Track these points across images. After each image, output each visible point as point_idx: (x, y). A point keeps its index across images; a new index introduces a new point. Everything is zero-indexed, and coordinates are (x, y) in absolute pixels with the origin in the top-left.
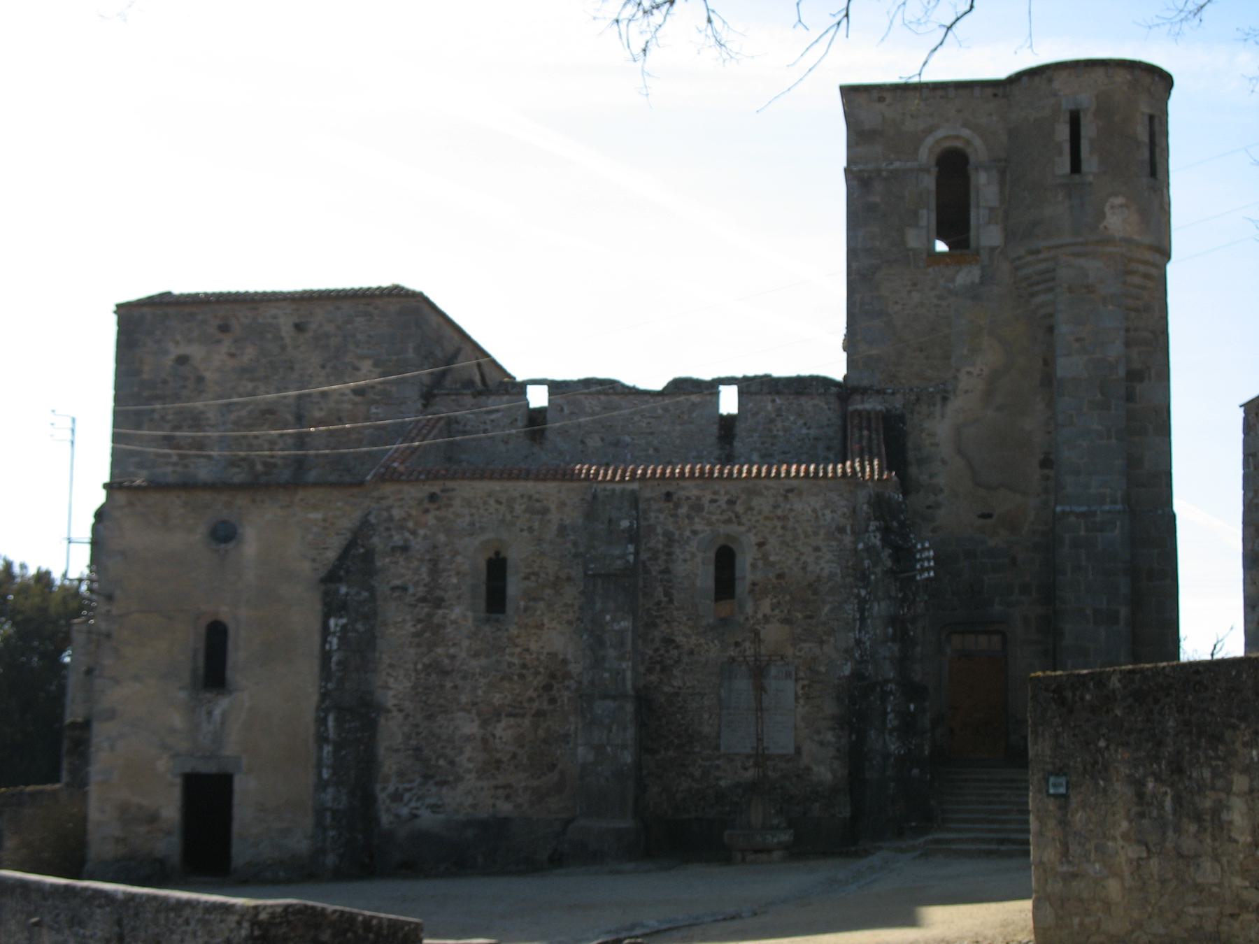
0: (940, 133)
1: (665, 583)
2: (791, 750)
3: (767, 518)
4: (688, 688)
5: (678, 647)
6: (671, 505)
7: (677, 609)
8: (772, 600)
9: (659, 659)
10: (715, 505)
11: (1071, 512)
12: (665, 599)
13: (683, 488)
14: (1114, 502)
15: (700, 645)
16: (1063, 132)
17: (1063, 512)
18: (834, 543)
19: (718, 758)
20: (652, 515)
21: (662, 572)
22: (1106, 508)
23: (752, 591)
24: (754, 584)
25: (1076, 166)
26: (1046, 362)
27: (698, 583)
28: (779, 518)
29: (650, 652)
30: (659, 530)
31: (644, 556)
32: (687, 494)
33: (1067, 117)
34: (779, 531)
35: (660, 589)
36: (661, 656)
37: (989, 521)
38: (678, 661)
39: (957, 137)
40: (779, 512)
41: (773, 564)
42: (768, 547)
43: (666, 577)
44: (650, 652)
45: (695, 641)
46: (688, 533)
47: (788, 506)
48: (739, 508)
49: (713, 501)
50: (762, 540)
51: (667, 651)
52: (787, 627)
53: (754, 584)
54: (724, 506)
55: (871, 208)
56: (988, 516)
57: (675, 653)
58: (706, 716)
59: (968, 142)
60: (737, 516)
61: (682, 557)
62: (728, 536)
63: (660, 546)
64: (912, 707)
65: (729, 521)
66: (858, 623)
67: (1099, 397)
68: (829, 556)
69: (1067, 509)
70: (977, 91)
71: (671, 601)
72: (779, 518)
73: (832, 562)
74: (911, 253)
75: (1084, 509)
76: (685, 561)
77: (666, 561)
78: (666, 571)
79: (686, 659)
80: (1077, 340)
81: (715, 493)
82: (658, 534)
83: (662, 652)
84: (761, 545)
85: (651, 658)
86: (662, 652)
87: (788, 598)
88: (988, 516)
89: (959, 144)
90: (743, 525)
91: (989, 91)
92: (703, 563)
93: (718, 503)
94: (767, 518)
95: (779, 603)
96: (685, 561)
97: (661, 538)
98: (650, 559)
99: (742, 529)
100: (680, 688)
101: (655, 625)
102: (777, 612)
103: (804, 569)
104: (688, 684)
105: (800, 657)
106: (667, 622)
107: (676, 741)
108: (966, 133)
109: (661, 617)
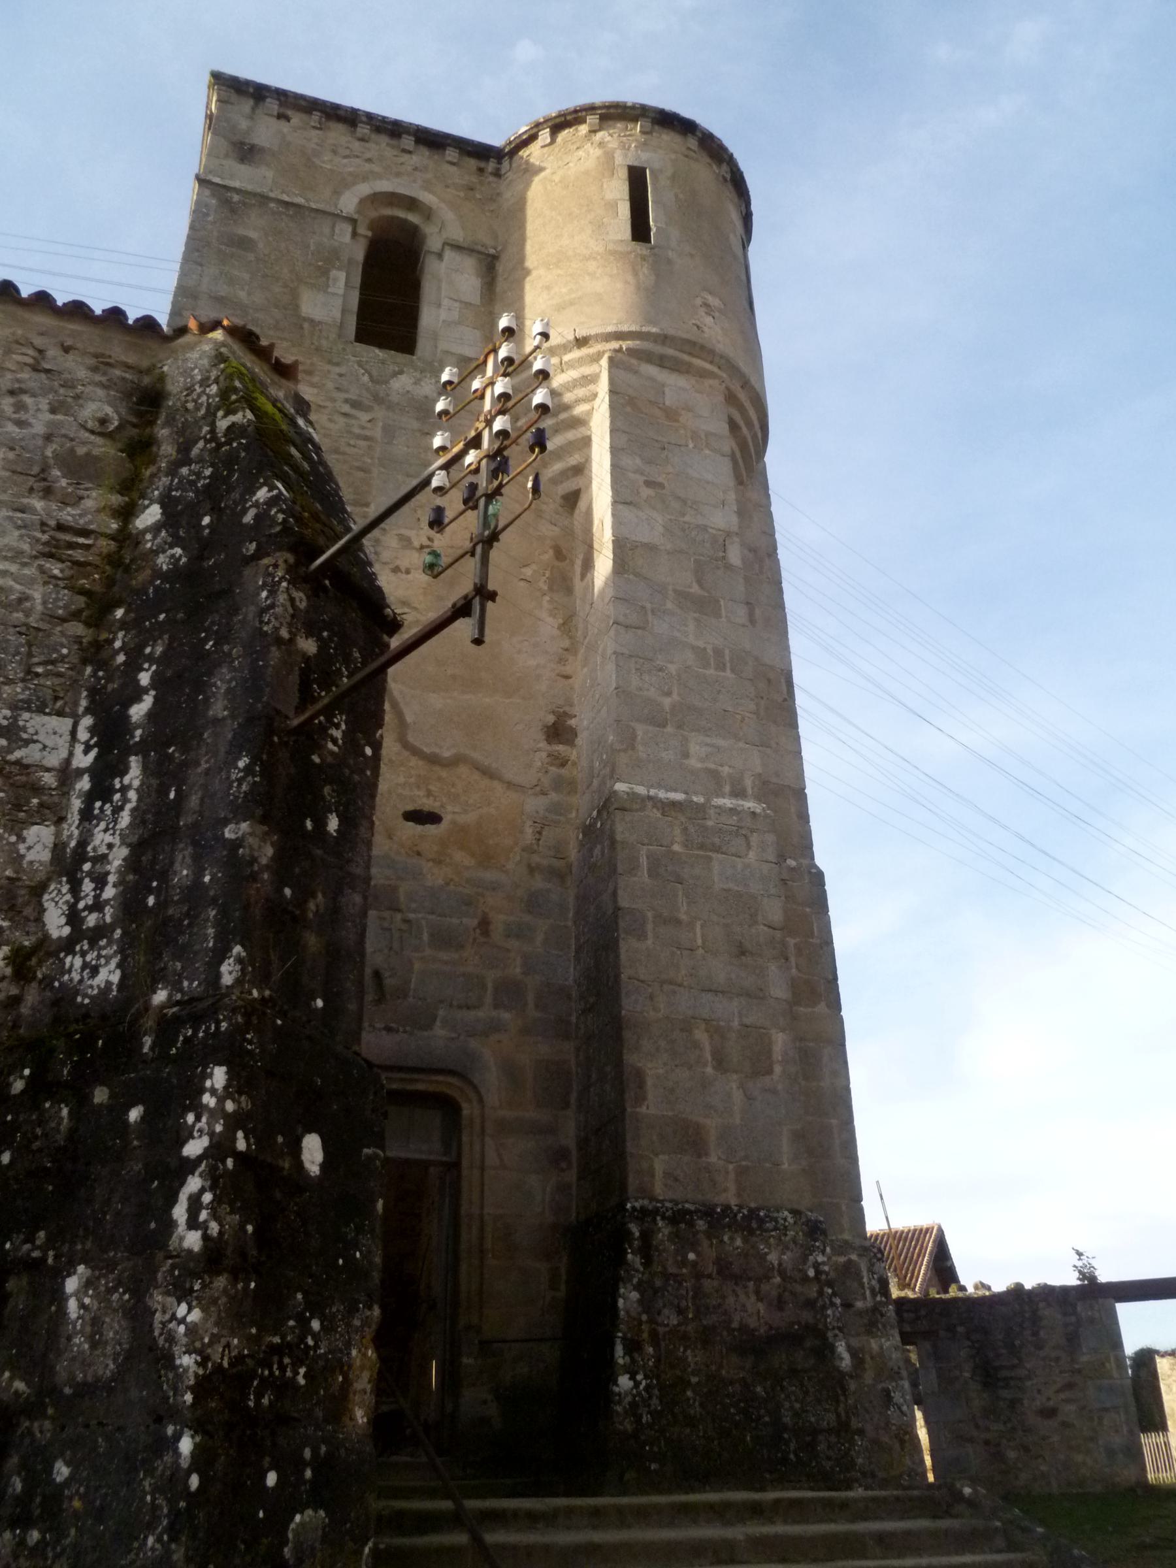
0: (385, 186)
11: (650, 798)
14: (739, 793)
16: (618, 190)
17: (633, 796)
18: (38, 504)
22: (728, 802)
25: (640, 230)
26: (559, 554)
33: (623, 174)
37: (431, 829)
39: (412, 204)
55: (244, 244)
56: (431, 818)
59: (428, 214)
64: (312, 1150)
66: (85, 784)
67: (695, 589)
69: (641, 790)
70: (451, 154)
74: (306, 325)
75: (678, 796)
80: (649, 484)
88: (431, 818)
89: (413, 218)
91: (473, 163)
108: (426, 198)
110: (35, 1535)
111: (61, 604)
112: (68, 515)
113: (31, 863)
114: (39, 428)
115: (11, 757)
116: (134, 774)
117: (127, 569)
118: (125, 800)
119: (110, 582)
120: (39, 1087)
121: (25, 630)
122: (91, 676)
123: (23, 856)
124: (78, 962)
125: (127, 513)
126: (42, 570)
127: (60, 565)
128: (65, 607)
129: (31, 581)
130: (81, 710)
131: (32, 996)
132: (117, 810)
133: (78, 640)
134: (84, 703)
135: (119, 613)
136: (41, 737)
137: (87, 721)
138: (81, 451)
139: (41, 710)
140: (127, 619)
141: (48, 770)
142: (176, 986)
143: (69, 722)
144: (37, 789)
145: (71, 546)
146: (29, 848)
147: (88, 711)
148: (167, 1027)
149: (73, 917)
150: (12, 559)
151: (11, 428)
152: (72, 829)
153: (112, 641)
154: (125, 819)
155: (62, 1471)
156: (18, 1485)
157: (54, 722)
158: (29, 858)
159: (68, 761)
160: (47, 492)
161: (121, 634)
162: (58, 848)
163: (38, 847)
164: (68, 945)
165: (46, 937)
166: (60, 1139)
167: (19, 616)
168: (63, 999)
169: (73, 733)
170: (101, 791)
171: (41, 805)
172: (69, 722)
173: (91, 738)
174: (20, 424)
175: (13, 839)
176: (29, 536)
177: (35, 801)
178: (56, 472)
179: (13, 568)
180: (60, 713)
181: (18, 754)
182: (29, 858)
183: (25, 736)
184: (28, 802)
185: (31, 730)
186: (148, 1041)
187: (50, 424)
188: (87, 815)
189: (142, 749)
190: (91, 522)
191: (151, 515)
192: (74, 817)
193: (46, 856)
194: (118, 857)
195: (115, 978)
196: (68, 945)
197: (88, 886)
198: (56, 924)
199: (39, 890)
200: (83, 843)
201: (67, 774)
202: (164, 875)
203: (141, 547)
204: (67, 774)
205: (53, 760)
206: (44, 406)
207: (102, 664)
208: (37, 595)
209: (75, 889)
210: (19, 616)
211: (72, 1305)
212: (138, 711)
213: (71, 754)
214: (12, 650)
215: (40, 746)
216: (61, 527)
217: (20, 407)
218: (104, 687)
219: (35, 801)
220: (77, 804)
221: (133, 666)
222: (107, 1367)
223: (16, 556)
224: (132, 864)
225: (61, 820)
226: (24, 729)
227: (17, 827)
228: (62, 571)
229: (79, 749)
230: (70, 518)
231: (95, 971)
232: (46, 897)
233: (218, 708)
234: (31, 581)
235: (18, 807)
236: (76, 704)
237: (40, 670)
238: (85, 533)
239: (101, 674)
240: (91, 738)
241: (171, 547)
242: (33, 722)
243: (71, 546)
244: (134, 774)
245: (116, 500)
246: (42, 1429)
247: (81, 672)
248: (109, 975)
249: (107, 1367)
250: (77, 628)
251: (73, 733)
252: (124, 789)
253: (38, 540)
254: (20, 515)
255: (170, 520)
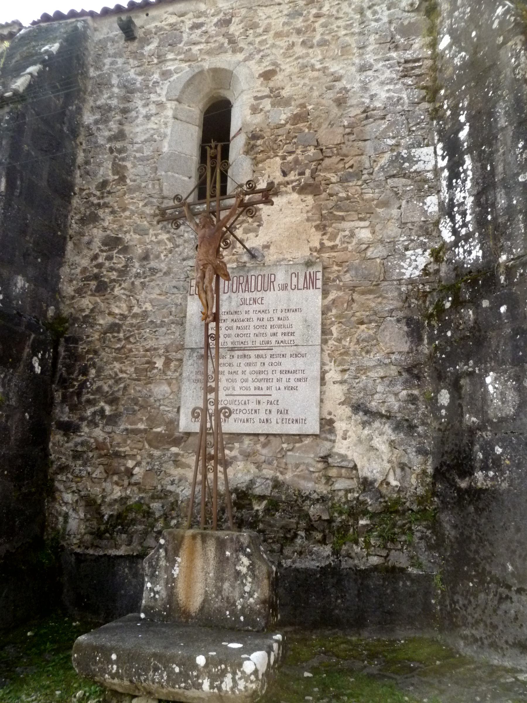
1: (115, 154)
2: (313, 427)
3: (278, 35)
4: (135, 316)
5: (125, 250)
6: (136, 44)
7: (131, 190)
8: (284, 158)
9: (96, 271)
10: (199, 31)
12: (111, 177)
13: (154, 19)
15: (159, 243)
18: (394, 54)
19: (177, 442)
20: (108, 61)
21: (110, 139)
23: (250, 149)
24: (255, 137)
27: (165, 149)
28: (299, 32)
29: (85, 262)
30: (115, 81)
31: (88, 118)
32: (159, 24)
34: (299, 50)
35: (109, 165)
36: (100, 266)
38: (123, 272)
40: (299, 23)
41: (287, 102)
42: (279, 77)
43: (118, 145)
44: (85, 262)
45: (154, 239)
46: (156, 77)
47: (314, 11)
48: (235, 29)
49: (196, 26)
50: (270, 68)
51: (109, 258)
52: (310, 199)
53: (255, 137)
54: (212, 30)
57: (119, 261)
58: (159, 363)
60: (232, 41)
61: (143, 111)
62: (216, 72)
63: (114, 102)
65: (220, 50)
66: (446, 173)
68: (388, 74)
71: (122, 179)
72: (299, 32)
73: (391, 81)
76: (148, 117)
77: (121, 124)
78: (120, 136)
79: (136, 268)
81: (201, 14)
82: (113, 86)
83: (100, 260)
84: (267, 75)
85: (85, 270)
86: (100, 260)
87: (312, 151)
90: (241, 50)
92: (175, 118)
93: (204, 29)
94: (278, 35)
95: (296, 161)
96: (148, 117)
97: (116, 90)
98: (96, 122)
99: (240, 57)
100: (124, 317)
101: (94, 219)
102: (292, 176)
103: (340, 102)
104: (136, 310)
105: (333, 248)
106: (113, 212)
107: (108, 410)
109: (106, 205)
110: (491, 474)
111: (415, 96)
112: (408, 55)
113: (431, 213)
114: (385, 19)
115: (412, 170)
116: (468, 163)
117: (441, 71)
118: (467, 176)
119: (435, 80)
120: (457, 303)
121: (403, 113)
122: (436, 125)
123: (427, 211)
124: (461, 250)
125: (434, 45)
126: (404, 84)
127: (411, 79)
128: (418, 97)
129: (401, 90)
130: (436, 141)
131: (444, 268)
132: (464, 181)
133: (427, 110)
134: (436, 138)
135: (442, 92)
136: (422, 158)
137: (440, 145)
138: (406, 23)
139: (419, 146)
140: (447, 93)
141: (428, 171)
142: (510, 252)
143: (432, 148)
144: (426, 181)
145: (413, 68)
146: (429, 207)
147: (439, 141)
148: (510, 271)
149: (455, 232)
150: (390, 83)
151: (373, 24)
152: (445, 194)
153: (443, 106)
154: (469, 184)
155: (499, 450)
156: (480, 455)
157: (425, 150)
158: (429, 211)
159: (436, 165)
160: (397, 48)
161: (446, 102)
162: (441, 204)
163: (432, 206)
164: (456, 244)
165: (444, 243)
166: (471, 324)
167: (399, 107)
168: (458, 267)
169: (435, 152)
170: (454, 174)
171: (429, 187)
172: (432, 148)
173: (444, 152)
174: (377, 20)
175: (421, 204)
176: (394, 70)
177: (426, 186)
178: (398, 37)
179: (392, 87)
180: (428, 145)
181: (414, 168)
182: (429, 211)
183: (415, 159)
184: (423, 187)
185: (417, 156)
186: (502, 278)
187: (389, 15)
188: (450, 186)
189: (469, 151)
190: (419, 54)
191: (445, 41)
192: (444, 189)
193: (436, 208)
194: (470, 201)
195: (480, 254)
196: (456, 244)
197: (458, 217)
198: (448, 236)
199: (437, 223)
200: (451, 200)
201: (437, 171)
202: (493, 205)
203: (444, 58)
204: (437, 171)
205: (430, 167)
206: (385, 8)
207: (441, 118)
208: (404, 96)
209: (453, 219)
210: (399, 107)
211: (491, 389)
212: (463, 135)
213: (436, 162)
214: (400, 124)
215: (422, 162)
216: (406, 62)
217: (375, 13)
218: (444, 128)
219: (426, 186)
220: (444, 183)
221: (456, 114)
222: (510, 411)
223: (391, 81)
224: (477, 203)
225: (439, 191)
226: (414, 156)
227: (422, 199)
228: (412, 81)
229: (439, 159)
230: (409, 56)
231: (470, 253)
232: (440, 226)
233: (503, 122)
234: (401, 90)
235: (420, 190)
236: (433, 139)
237: (414, 129)
238: (417, 60)
239: (441, 122)
240: (444, 152)
241: (459, 53)
242: (417, 152)
243: (413, 68)
244: (468, 163)
245: (428, 39)
246: (488, 435)
247: (432, 124)
248: (477, 253)
249: (510, 411)
250: (425, 105)
251: (435, 152)
252: (465, 171)
253: (398, 71)
254: (387, 62)
255: (456, 40)
